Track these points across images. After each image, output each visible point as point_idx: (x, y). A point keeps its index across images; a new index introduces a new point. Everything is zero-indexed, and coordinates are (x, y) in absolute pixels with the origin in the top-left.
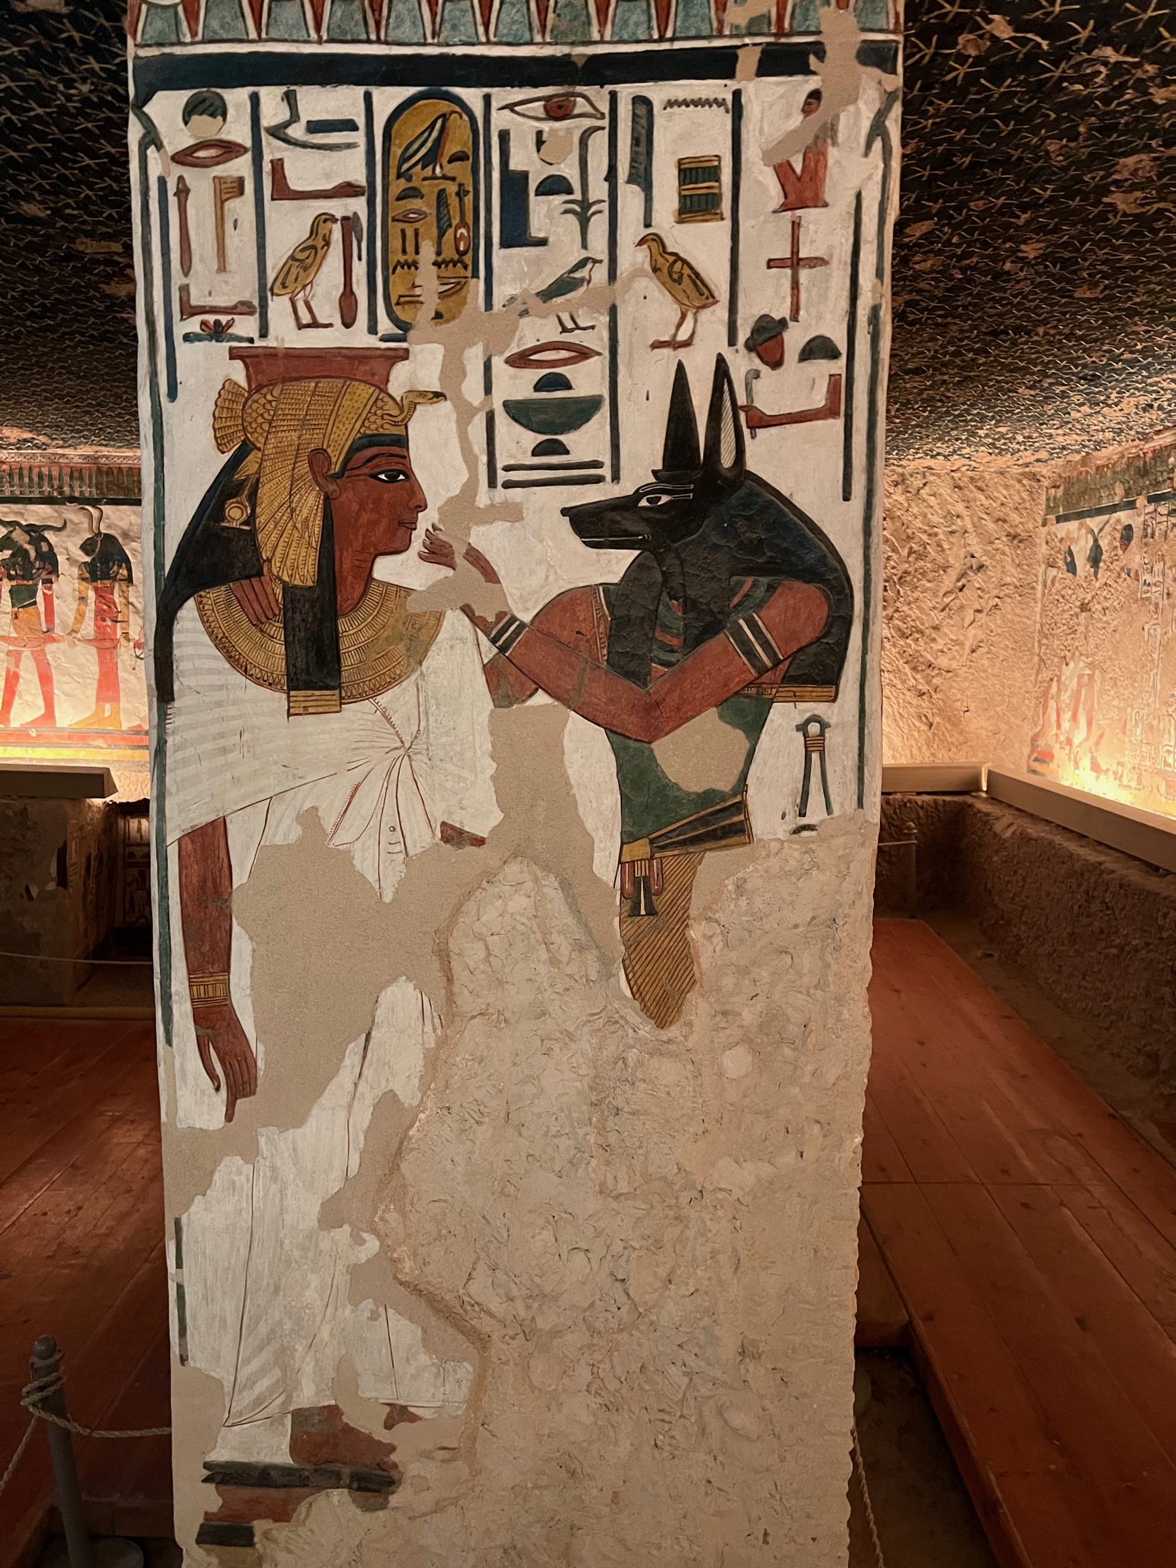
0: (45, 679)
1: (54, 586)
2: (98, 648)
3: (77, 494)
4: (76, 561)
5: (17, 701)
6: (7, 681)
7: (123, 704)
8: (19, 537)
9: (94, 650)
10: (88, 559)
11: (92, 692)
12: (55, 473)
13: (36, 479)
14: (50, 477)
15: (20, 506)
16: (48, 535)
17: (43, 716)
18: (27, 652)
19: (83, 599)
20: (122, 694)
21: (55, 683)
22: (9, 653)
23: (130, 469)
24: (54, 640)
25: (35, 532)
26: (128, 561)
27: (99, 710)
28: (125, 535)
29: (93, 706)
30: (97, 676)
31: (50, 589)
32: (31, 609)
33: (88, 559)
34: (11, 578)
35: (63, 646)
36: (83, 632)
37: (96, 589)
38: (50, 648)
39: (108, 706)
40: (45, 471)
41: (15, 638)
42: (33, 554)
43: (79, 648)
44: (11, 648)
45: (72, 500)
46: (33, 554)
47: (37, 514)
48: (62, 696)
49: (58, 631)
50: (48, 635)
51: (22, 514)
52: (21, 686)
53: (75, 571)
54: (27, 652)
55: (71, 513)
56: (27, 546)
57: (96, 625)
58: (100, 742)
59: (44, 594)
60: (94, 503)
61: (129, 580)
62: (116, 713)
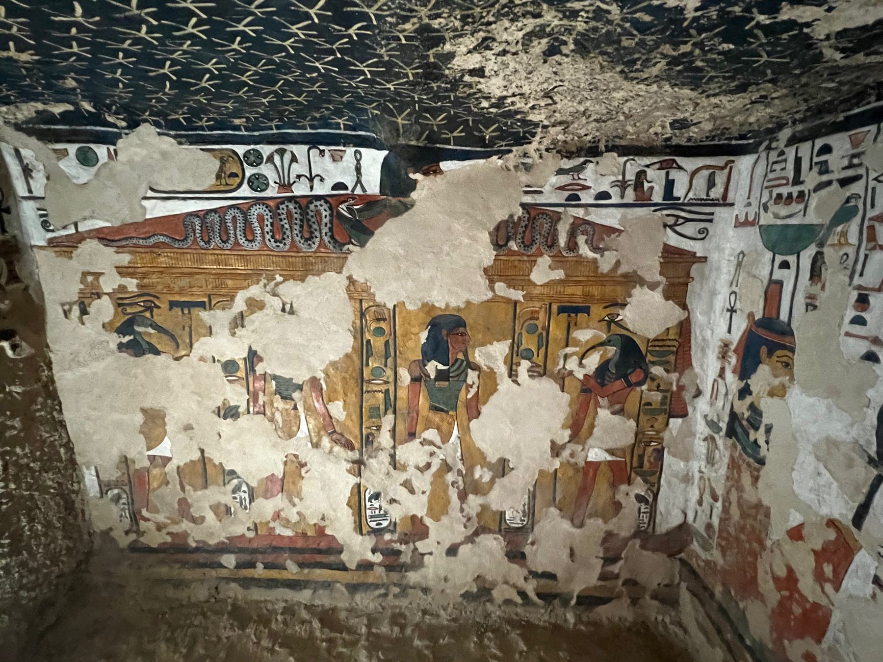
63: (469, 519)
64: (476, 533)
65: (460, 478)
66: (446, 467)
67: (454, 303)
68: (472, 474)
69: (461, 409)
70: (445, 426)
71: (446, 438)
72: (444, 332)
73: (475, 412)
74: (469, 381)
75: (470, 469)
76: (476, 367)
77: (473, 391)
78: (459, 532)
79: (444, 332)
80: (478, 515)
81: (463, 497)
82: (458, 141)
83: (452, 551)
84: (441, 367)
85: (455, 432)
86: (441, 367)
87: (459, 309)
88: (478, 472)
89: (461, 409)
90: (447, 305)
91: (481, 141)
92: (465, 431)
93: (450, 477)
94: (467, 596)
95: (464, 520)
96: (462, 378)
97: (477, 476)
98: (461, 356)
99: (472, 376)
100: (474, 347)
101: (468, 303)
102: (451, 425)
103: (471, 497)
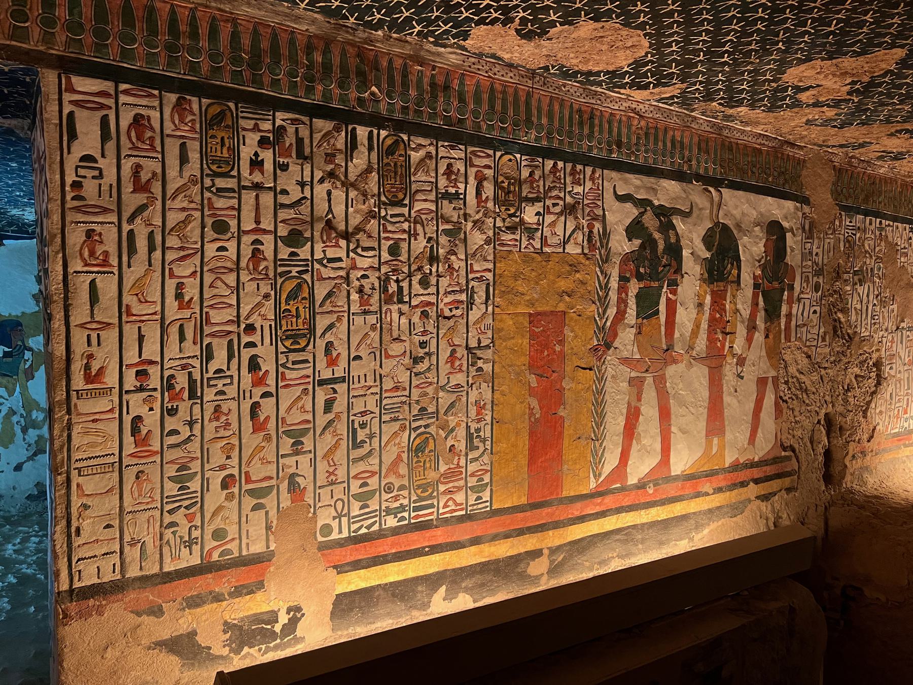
0: (665, 414)
1: (679, 288)
2: (710, 367)
3: (701, 172)
4: (699, 256)
5: (635, 447)
6: (627, 418)
7: (729, 436)
8: (650, 221)
9: (706, 370)
10: (708, 255)
11: (702, 425)
12: (686, 141)
13: (669, 145)
14: (682, 143)
15: (652, 180)
16: (677, 221)
17: (660, 464)
18: (649, 380)
19: (700, 305)
20: (726, 423)
21: (673, 417)
22: (631, 381)
23: (745, 146)
24: (675, 361)
25: (664, 215)
26: (739, 260)
27: (709, 444)
28: (738, 226)
29: (704, 440)
30: (706, 404)
31: (674, 292)
32: (653, 320)
33: (708, 255)
34: (640, 277)
35: (681, 367)
36: (698, 348)
37: (713, 294)
38: (671, 370)
39: (715, 441)
40: (678, 135)
41: (638, 361)
42: (661, 245)
43: (695, 368)
44: (633, 374)
45: (698, 177)
46: (661, 245)
47: (668, 192)
48: (679, 434)
49: (679, 348)
50: (668, 355)
51: (655, 190)
52: (640, 428)
53: (698, 268)
54: (649, 380)
55: (696, 195)
56: (657, 235)
57: (708, 339)
58: (707, 487)
59: (668, 299)
60: (717, 183)
61: (738, 281)
62: (722, 447)
63: (30, 445)
64: (35, 454)
65: (22, 419)
66: (12, 412)
67: (14, 314)
68: (31, 416)
69: (21, 375)
70: (11, 386)
71: (11, 393)
72: (8, 329)
73: (30, 376)
74: (26, 358)
75: (29, 413)
76: (30, 349)
77: (28, 364)
78: (23, 454)
79: (8, 329)
80: (36, 442)
81: (24, 430)
82: (13, 231)
83: (18, 468)
84: (7, 349)
85: (18, 389)
86: (7, 349)
87: (17, 316)
88: (34, 414)
89: (21, 375)
90: (10, 314)
91: (27, 233)
92: (24, 388)
93: (15, 419)
94: (29, 497)
95: (26, 446)
96: (21, 355)
97: (34, 417)
98: (20, 343)
99: (28, 355)
100: (28, 337)
101: (23, 313)
102: (15, 385)
103: (30, 431)
